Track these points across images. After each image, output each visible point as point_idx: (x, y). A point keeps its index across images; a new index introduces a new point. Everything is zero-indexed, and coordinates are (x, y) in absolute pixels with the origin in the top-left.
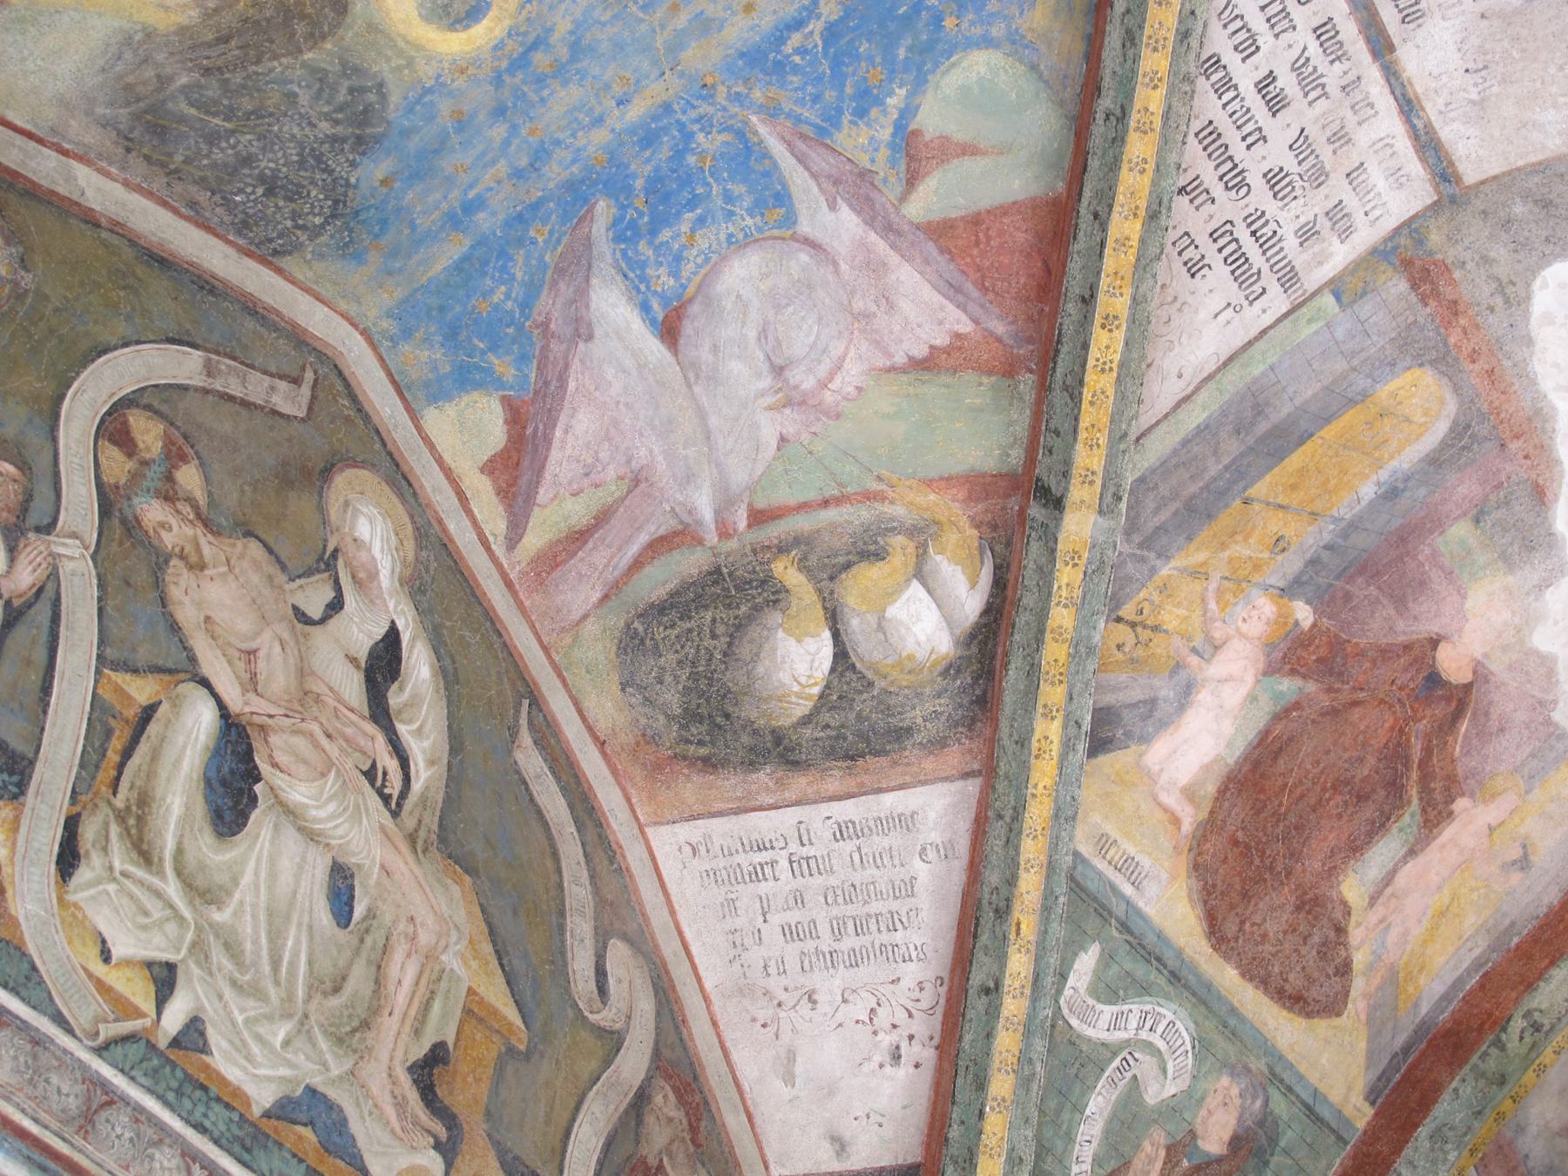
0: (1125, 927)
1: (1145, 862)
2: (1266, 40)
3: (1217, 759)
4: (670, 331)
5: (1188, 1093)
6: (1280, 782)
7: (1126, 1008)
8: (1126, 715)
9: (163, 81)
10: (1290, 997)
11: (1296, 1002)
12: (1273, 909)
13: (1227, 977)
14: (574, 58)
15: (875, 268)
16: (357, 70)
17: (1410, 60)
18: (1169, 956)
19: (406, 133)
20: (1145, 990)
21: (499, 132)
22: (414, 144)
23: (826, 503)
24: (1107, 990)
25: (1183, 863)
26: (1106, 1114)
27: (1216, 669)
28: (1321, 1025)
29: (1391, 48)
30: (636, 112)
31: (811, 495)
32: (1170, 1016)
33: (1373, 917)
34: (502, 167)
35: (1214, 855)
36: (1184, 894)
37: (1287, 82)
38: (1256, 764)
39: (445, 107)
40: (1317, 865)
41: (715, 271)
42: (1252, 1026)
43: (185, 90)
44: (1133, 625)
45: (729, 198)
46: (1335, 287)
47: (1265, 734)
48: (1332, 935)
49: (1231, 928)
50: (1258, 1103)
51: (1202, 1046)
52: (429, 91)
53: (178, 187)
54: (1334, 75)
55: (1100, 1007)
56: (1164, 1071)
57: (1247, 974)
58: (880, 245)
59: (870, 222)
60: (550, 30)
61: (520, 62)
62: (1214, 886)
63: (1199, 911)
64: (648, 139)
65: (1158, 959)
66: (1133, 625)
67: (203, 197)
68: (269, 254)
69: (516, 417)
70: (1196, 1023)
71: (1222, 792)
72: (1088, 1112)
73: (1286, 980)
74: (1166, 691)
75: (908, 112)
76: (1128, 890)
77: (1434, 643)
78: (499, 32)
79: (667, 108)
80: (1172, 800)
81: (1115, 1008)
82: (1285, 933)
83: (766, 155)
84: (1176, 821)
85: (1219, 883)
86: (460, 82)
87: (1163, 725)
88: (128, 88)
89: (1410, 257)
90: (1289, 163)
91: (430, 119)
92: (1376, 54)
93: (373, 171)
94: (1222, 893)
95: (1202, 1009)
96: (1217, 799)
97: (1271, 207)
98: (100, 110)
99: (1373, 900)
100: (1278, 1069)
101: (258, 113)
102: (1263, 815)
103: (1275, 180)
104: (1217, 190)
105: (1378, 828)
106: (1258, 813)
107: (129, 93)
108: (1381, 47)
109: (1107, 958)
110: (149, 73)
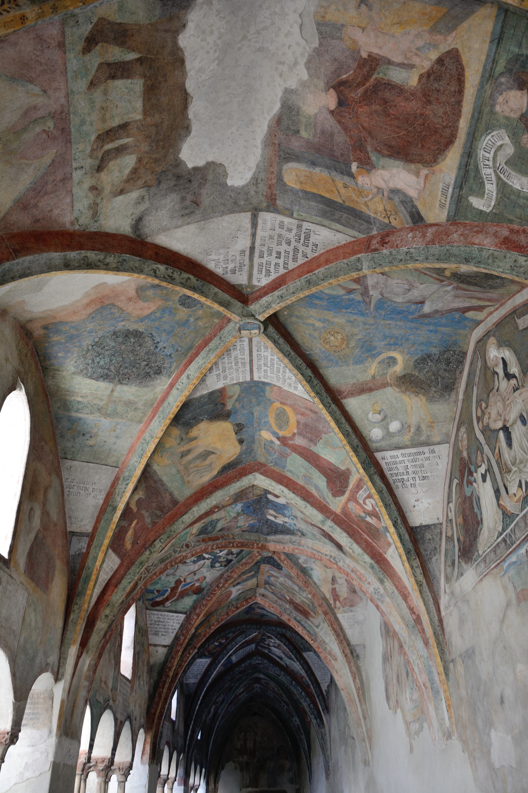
0: (461, 188)
1: (441, 185)
2: (273, 263)
3: (404, 169)
4: (422, 303)
5: (506, 127)
6: (398, 140)
7: (484, 177)
8: (409, 210)
9: (435, 392)
10: (460, 85)
11: (460, 80)
12: (435, 115)
13: (463, 124)
14: (388, 336)
15: (374, 287)
16: (415, 366)
17: (248, 244)
18: (464, 163)
19: (422, 351)
20: (477, 170)
21: (412, 337)
22: (424, 348)
23: (426, 274)
24: (480, 192)
25: (437, 168)
26: (520, 176)
27: (382, 185)
28: (465, 58)
29: (250, 247)
30: (389, 322)
31: (427, 276)
32: (482, 152)
33: (416, 61)
34: (418, 332)
35: (429, 155)
36: (444, 163)
37: (274, 254)
38: (398, 153)
39: (412, 349)
40: (414, 102)
41: (403, 303)
42: (475, 102)
43: (436, 388)
44: (389, 218)
45: (389, 306)
46: (291, 216)
47: (390, 156)
48: (432, 78)
49: (448, 131)
50: (503, 80)
51: (489, 128)
52: (411, 354)
53: (458, 377)
54: (265, 249)
55: (487, 192)
56: (501, 146)
57: (458, 114)
58: (370, 288)
59: (368, 290)
60: (385, 345)
61: (395, 344)
62: (438, 149)
63: (446, 153)
64: (392, 319)
65: (466, 166)
66: (389, 218)
67: (458, 372)
68: (465, 354)
69: (464, 312)
70: (481, 136)
71: (411, 161)
72: (519, 188)
73: (455, 91)
74: (397, 200)
75: (344, 295)
76: (451, 190)
77: (332, 112)
78: (391, 352)
79: (384, 319)
80: (422, 181)
81: (486, 182)
82: (440, 103)
83: (375, 306)
84: (426, 176)
85: (436, 147)
86: (406, 350)
87: (405, 195)
88: (440, 396)
89: (272, 206)
90: (283, 243)
91: (417, 350)
92: (254, 248)
93: (434, 351)
94: (438, 144)
95: (476, 134)
96: (415, 162)
97: (293, 240)
98: (447, 397)
99: (412, 66)
100: (487, 75)
101: (434, 375)
102: (410, 140)
103: (289, 243)
104: (300, 252)
105: (390, 86)
106: (410, 142)
107: (442, 396)
108: (252, 249)
109: (472, 192)
110: (435, 395)
